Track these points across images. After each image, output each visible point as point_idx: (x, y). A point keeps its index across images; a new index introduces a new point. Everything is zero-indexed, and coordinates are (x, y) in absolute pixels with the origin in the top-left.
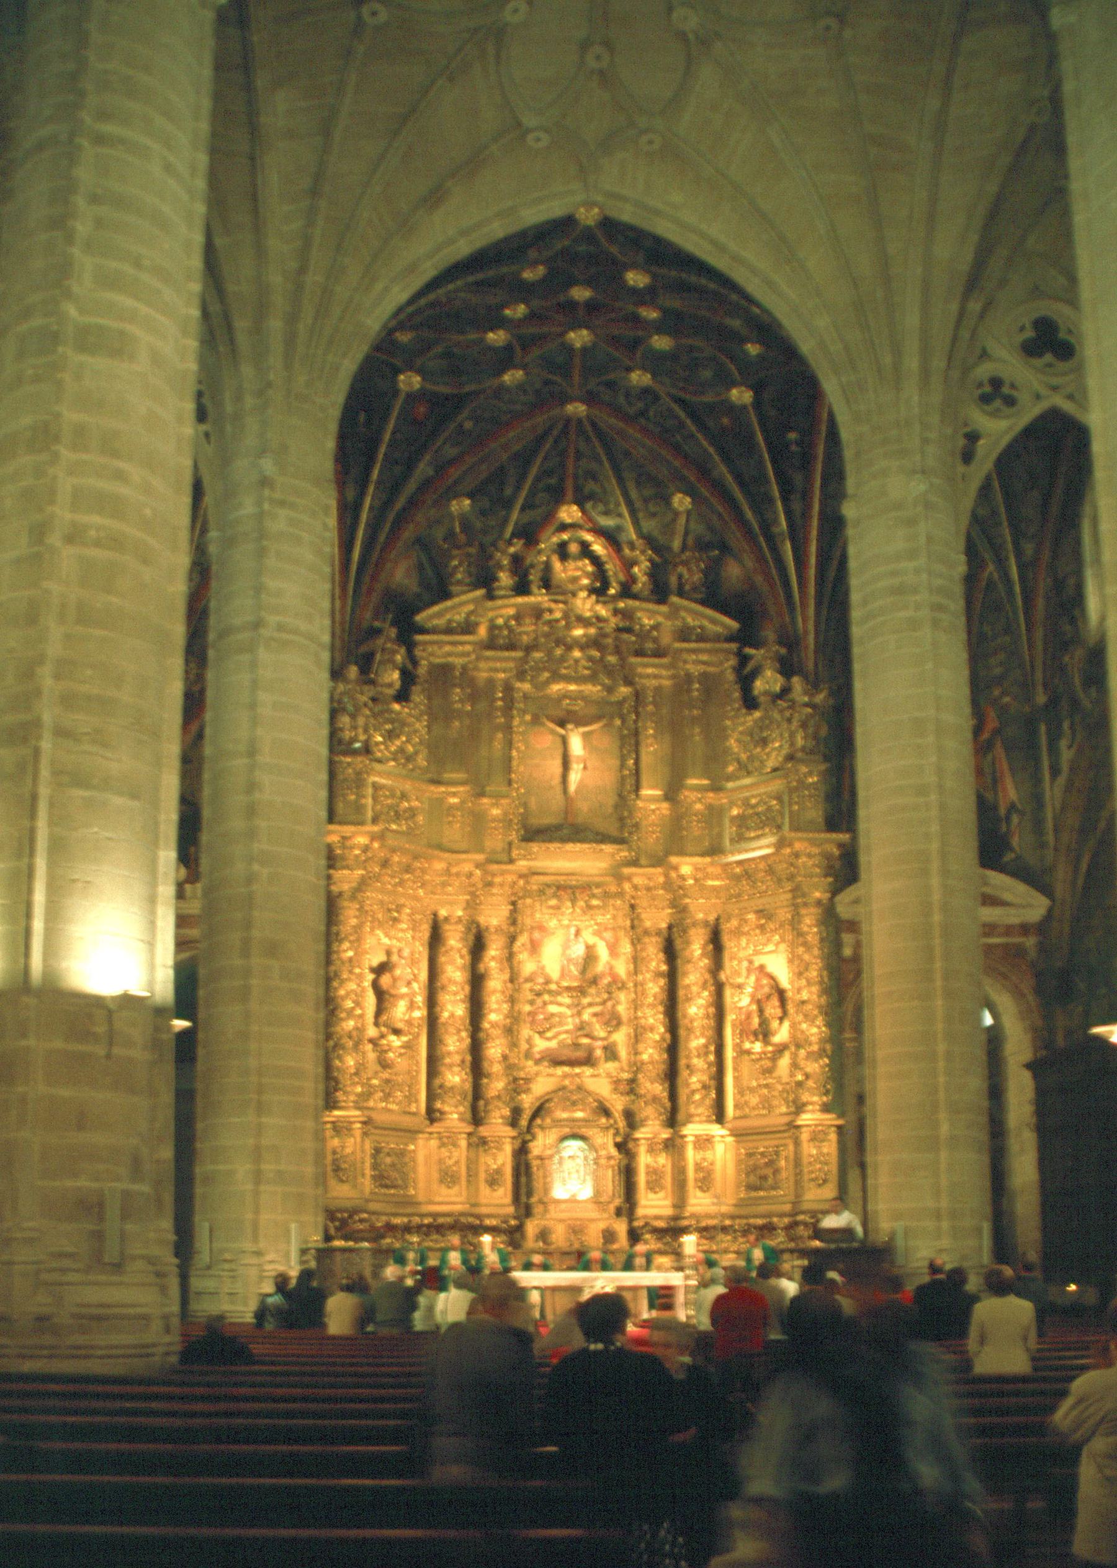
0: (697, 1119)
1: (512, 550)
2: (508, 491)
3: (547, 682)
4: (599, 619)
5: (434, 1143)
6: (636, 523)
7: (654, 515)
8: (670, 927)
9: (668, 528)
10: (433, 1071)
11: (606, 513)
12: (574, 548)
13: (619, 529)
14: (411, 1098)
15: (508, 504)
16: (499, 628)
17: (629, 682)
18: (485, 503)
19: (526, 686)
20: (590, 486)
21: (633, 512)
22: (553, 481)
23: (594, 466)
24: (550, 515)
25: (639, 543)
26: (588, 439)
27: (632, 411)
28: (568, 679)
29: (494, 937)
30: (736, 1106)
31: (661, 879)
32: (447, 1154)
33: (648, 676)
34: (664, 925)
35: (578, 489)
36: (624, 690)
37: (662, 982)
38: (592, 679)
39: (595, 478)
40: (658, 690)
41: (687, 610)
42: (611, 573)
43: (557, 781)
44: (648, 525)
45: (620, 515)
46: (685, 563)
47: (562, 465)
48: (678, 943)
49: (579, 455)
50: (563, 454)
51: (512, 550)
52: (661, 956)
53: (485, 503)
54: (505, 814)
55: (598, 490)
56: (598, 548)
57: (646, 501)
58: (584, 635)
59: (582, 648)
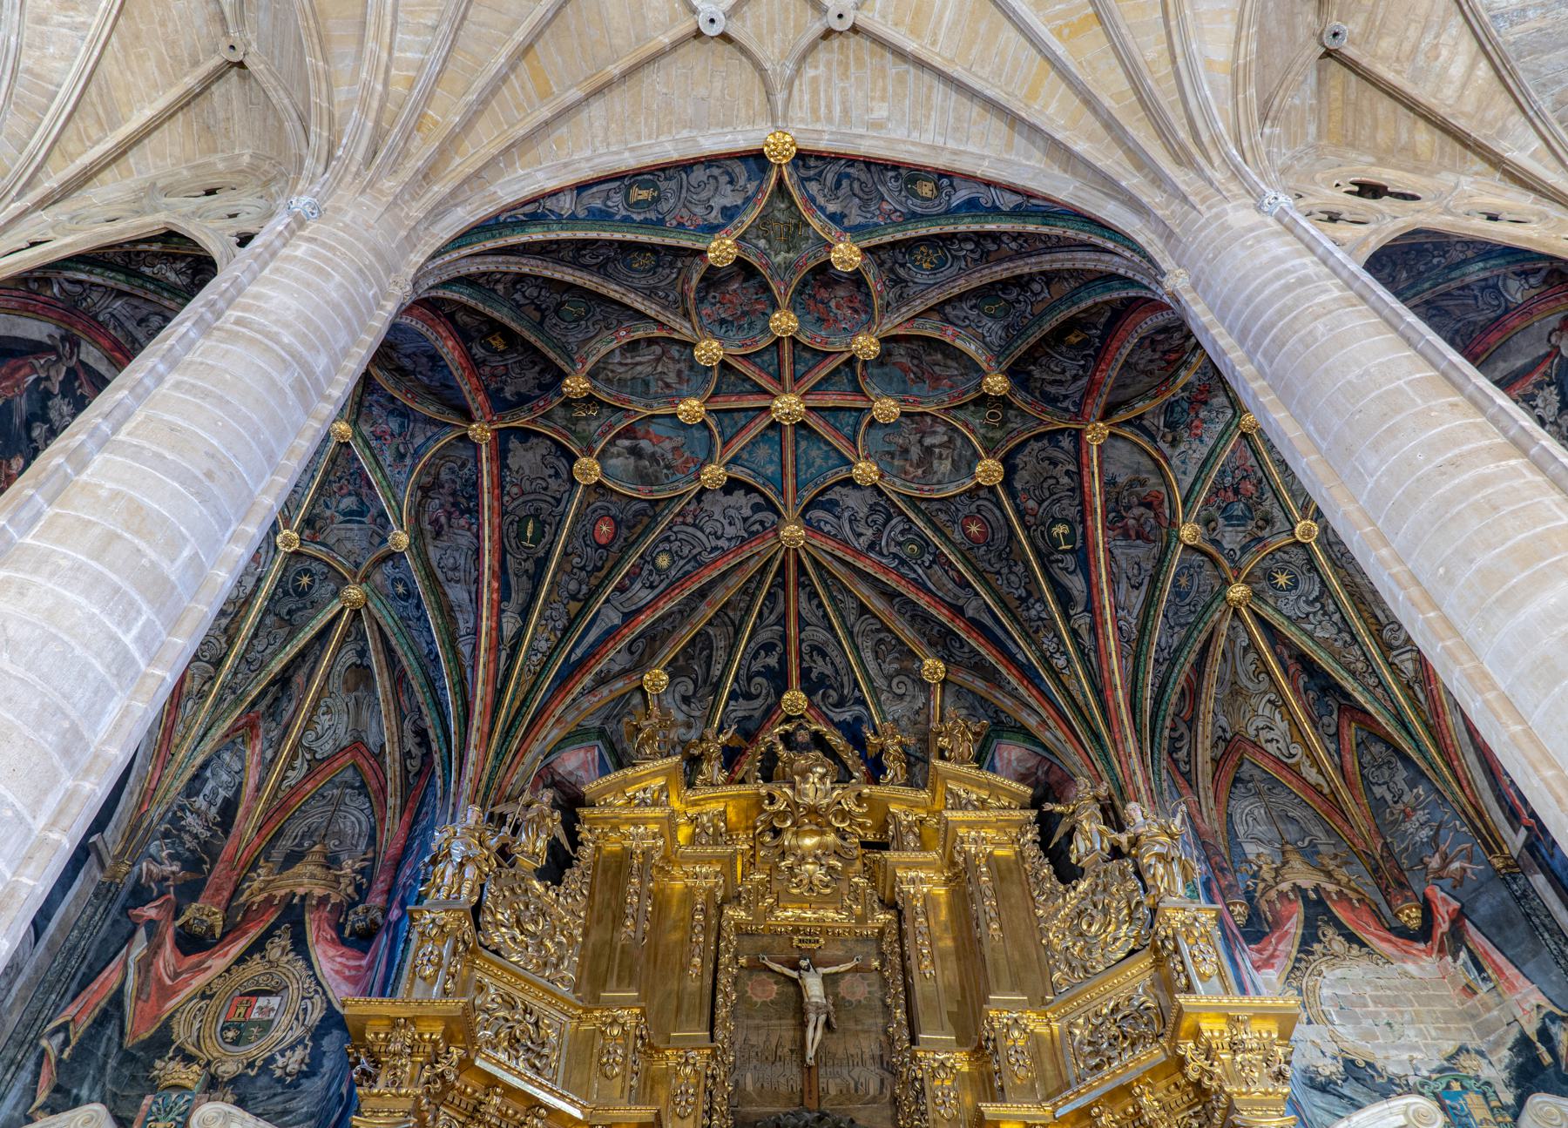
1: (723, 738)
2: (716, 670)
3: (771, 910)
6: (878, 704)
7: (901, 697)
11: (840, 704)
13: (858, 720)
15: (717, 687)
18: (687, 686)
20: (820, 667)
21: (875, 692)
22: (772, 661)
23: (821, 635)
26: (814, 595)
27: (863, 543)
28: (799, 900)
33: (913, 881)
35: (805, 674)
36: (882, 917)
38: (834, 900)
39: (824, 655)
41: (958, 778)
46: (949, 734)
47: (784, 638)
49: (802, 623)
50: (783, 619)
51: (723, 738)
53: (687, 686)
55: (829, 671)
56: (835, 739)
57: (889, 678)
58: (819, 846)
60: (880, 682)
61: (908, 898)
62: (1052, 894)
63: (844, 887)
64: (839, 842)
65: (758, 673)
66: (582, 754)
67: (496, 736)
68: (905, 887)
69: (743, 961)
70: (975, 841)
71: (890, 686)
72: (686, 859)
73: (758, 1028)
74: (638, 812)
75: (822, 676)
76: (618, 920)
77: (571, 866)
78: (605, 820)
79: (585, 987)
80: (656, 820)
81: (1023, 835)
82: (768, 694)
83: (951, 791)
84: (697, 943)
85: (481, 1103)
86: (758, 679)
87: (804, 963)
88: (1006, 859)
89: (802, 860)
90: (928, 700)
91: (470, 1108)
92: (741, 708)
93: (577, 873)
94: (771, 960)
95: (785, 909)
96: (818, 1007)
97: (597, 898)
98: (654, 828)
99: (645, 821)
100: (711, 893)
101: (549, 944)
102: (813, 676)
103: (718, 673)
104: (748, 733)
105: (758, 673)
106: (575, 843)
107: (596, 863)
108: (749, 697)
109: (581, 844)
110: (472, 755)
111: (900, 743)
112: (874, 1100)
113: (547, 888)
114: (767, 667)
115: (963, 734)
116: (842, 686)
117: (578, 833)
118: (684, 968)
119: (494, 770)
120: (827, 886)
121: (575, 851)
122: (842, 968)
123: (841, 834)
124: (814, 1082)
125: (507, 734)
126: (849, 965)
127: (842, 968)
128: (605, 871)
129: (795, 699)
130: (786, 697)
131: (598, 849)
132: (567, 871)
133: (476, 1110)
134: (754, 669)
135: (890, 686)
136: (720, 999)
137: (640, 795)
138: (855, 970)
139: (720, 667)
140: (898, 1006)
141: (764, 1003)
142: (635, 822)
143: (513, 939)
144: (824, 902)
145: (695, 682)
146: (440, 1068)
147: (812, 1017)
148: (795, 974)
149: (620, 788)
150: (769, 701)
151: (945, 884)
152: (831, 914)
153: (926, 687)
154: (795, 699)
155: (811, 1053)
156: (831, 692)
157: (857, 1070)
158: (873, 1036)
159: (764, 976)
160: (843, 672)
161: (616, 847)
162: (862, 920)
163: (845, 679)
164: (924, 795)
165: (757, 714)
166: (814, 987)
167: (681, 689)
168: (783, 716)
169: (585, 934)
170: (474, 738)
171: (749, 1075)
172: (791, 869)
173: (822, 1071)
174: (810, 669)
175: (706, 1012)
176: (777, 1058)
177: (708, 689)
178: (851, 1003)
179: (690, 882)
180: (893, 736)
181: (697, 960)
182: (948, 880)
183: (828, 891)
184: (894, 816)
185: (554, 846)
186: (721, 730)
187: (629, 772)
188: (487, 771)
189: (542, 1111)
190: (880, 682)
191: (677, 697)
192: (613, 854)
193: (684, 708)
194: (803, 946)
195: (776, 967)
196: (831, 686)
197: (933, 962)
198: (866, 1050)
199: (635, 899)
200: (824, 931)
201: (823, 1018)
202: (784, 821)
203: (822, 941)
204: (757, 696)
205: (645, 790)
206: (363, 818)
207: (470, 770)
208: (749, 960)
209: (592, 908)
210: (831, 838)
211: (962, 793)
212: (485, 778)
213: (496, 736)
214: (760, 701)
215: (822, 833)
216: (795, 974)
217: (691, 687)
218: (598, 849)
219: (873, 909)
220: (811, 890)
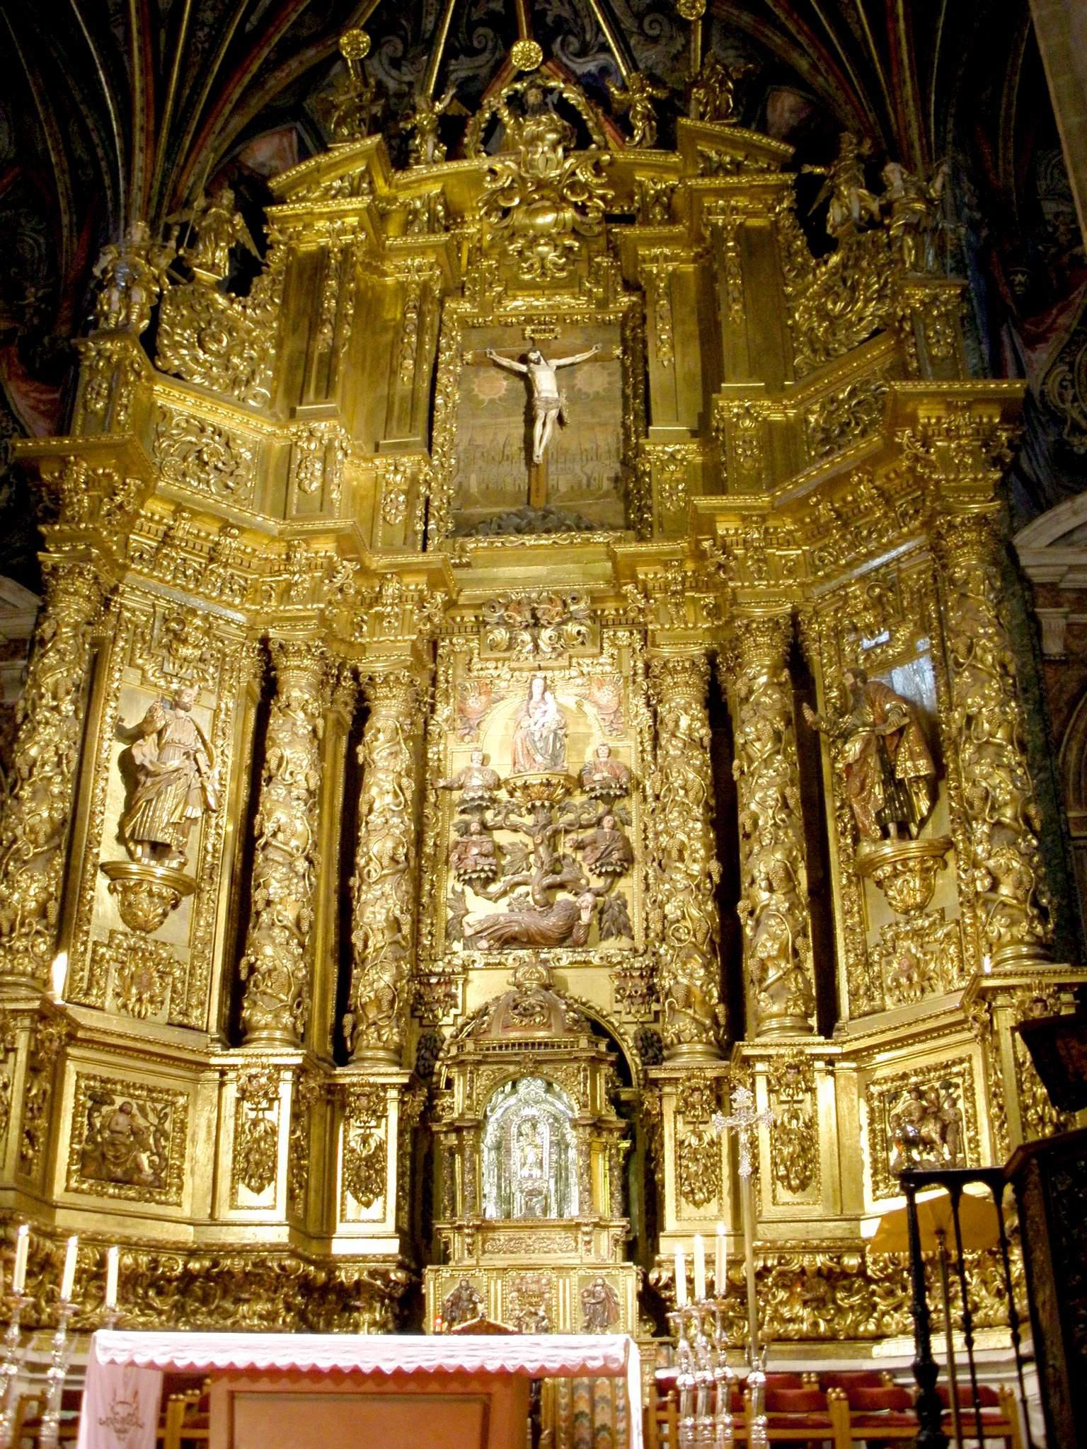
0: (774, 1023)
1: (439, 107)
2: (429, 23)
3: (499, 299)
4: (575, 187)
5: (231, 1092)
6: (627, 52)
7: (655, 40)
8: (711, 657)
9: (681, 57)
10: (238, 942)
11: (583, 52)
12: (533, 97)
13: (605, 71)
14: (184, 994)
16: (415, 213)
17: (631, 286)
18: (395, 46)
19: (465, 307)
24: (501, 63)
25: (633, 80)
28: (530, 287)
29: (382, 691)
30: (854, 995)
31: (690, 566)
32: (252, 1115)
33: (655, 259)
34: (696, 650)
36: (625, 300)
37: (700, 758)
38: (572, 284)
40: (674, 277)
42: (590, 124)
43: (518, 443)
44: (649, 56)
45: (605, 48)
48: (725, 677)
51: (439, 107)
52: (698, 711)
54: (414, 481)
56: (573, 96)
57: (639, 17)
58: (556, 223)
59: (552, 241)
60: (628, 23)
61: (650, 278)
62: (803, 271)
63: (582, 269)
64: (578, 217)
65: (481, 23)
66: (276, 140)
67: (164, 133)
68: (647, 267)
69: (469, 356)
70: (723, 211)
71: (640, 26)
72: (398, 250)
73: (483, 427)
74: (333, 206)
75: (559, 20)
76: (314, 328)
77: (259, 273)
78: (297, 217)
79: (281, 403)
80: (355, 212)
81: (780, 201)
82: (495, 48)
83: (702, 154)
84: (409, 344)
85: (170, 528)
86: (481, 30)
87: (533, 356)
88: (759, 230)
89: (533, 242)
90: (688, 42)
91: (161, 534)
92: (462, 68)
93: (266, 280)
94: (499, 354)
95: (515, 298)
96: (547, 401)
97: (292, 306)
98: (352, 220)
99: (342, 214)
100: (425, 288)
101: (236, 360)
102: (549, 20)
103: (430, 26)
104: (471, 97)
105: (481, 23)
106: (264, 245)
107: (289, 268)
108: (472, 52)
109: (271, 247)
110: (139, 160)
111: (651, 98)
112: (606, 495)
113: (232, 301)
114: (491, 13)
115: (722, 83)
116: (584, 31)
117: (267, 235)
118: (393, 373)
119: (166, 174)
120: (562, 269)
121: (264, 256)
122: (578, 358)
123: (582, 209)
124: (542, 479)
125: (177, 132)
126: (586, 355)
127: (578, 358)
128: (300, 275)
129: (525, 51)
130: (515, 49)
131: (291, 251)
132: (255, 280)
133: (166, 535)
134: (475, 17)
135: (640, 26)
136: (439, 400)
137: (337, 184)
138: (594, 359)
139: (432, 18)
140: (635, 397)
141: (492, 401)
142: (331, 217)
143: (196, 359)
144: (557, 286)
145: (404, 40)
146: (118, 499)
147: (541, 414)
148: (523, 368)
149: (309, 180)
150: (497, 55)
151: (694, 261)
152: (567, 299)
153: (685, 26)
154: (525, 51)
155: (539, 451)
156: (571, 39)
157: (590, 465)
158: (611, 429)
159: (493, 372)
160: (583, 13)
161: (312, 247)
162: (602, 304)
163: (586, 21)
164: (675, 159)
165: (484, 72)
166: (546, 381)
167: (387, 50)
168: (514, 73)
169: (279, 346)
170: (139, 139)
171: (473, 477)
172: (520, 253)
173: (552, 468)
174: (544, 12)
175: (422, 415)
176: (506, 458)
177: (420, 48)
178: (588, 395)
179: (402, 277)
180: (642, 90)
181: (409, 363)
182: (699, 256)
183: (564, 274)
184: (641, 184)
185: (238, 255)
186: (437, 96)
187: (323, 159)
188: (159, 176)
189: (235, 532)
190: (628, 23)
191: (385, 61)
192: (310, 255)
193: (394, 73)
194: (537, 336)
195: (505, 362)
196: (571, 32)
197: (673, 347)
198: (602, 443)
199: (333, 303)
200: (561, 319)
201: (553, 413)
202: (511, 199)
203: (558, 329)
204: (483, 50)
205: (342, 179)
206: (42, 240)
207: (138, 178)
208: (475, 355)
209: (286, 316)
210: (569, 214)
211: (713, 154)
212: (156, 185)
213: (164, 133)
214: (486, 56)
215: (558, 210)
216: (523, 368)
217: (400, 47)
218: (291, 251)
219: (616, 292)
220: (544, 274)
